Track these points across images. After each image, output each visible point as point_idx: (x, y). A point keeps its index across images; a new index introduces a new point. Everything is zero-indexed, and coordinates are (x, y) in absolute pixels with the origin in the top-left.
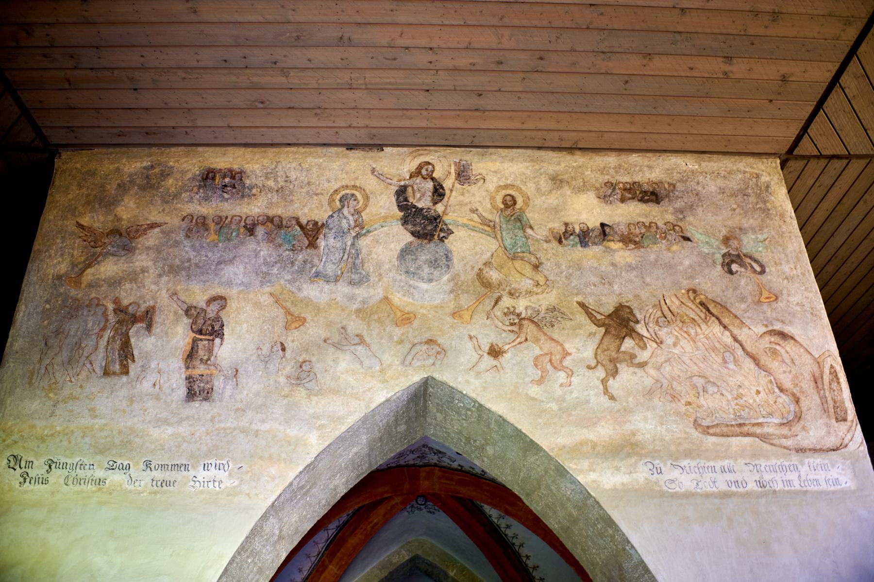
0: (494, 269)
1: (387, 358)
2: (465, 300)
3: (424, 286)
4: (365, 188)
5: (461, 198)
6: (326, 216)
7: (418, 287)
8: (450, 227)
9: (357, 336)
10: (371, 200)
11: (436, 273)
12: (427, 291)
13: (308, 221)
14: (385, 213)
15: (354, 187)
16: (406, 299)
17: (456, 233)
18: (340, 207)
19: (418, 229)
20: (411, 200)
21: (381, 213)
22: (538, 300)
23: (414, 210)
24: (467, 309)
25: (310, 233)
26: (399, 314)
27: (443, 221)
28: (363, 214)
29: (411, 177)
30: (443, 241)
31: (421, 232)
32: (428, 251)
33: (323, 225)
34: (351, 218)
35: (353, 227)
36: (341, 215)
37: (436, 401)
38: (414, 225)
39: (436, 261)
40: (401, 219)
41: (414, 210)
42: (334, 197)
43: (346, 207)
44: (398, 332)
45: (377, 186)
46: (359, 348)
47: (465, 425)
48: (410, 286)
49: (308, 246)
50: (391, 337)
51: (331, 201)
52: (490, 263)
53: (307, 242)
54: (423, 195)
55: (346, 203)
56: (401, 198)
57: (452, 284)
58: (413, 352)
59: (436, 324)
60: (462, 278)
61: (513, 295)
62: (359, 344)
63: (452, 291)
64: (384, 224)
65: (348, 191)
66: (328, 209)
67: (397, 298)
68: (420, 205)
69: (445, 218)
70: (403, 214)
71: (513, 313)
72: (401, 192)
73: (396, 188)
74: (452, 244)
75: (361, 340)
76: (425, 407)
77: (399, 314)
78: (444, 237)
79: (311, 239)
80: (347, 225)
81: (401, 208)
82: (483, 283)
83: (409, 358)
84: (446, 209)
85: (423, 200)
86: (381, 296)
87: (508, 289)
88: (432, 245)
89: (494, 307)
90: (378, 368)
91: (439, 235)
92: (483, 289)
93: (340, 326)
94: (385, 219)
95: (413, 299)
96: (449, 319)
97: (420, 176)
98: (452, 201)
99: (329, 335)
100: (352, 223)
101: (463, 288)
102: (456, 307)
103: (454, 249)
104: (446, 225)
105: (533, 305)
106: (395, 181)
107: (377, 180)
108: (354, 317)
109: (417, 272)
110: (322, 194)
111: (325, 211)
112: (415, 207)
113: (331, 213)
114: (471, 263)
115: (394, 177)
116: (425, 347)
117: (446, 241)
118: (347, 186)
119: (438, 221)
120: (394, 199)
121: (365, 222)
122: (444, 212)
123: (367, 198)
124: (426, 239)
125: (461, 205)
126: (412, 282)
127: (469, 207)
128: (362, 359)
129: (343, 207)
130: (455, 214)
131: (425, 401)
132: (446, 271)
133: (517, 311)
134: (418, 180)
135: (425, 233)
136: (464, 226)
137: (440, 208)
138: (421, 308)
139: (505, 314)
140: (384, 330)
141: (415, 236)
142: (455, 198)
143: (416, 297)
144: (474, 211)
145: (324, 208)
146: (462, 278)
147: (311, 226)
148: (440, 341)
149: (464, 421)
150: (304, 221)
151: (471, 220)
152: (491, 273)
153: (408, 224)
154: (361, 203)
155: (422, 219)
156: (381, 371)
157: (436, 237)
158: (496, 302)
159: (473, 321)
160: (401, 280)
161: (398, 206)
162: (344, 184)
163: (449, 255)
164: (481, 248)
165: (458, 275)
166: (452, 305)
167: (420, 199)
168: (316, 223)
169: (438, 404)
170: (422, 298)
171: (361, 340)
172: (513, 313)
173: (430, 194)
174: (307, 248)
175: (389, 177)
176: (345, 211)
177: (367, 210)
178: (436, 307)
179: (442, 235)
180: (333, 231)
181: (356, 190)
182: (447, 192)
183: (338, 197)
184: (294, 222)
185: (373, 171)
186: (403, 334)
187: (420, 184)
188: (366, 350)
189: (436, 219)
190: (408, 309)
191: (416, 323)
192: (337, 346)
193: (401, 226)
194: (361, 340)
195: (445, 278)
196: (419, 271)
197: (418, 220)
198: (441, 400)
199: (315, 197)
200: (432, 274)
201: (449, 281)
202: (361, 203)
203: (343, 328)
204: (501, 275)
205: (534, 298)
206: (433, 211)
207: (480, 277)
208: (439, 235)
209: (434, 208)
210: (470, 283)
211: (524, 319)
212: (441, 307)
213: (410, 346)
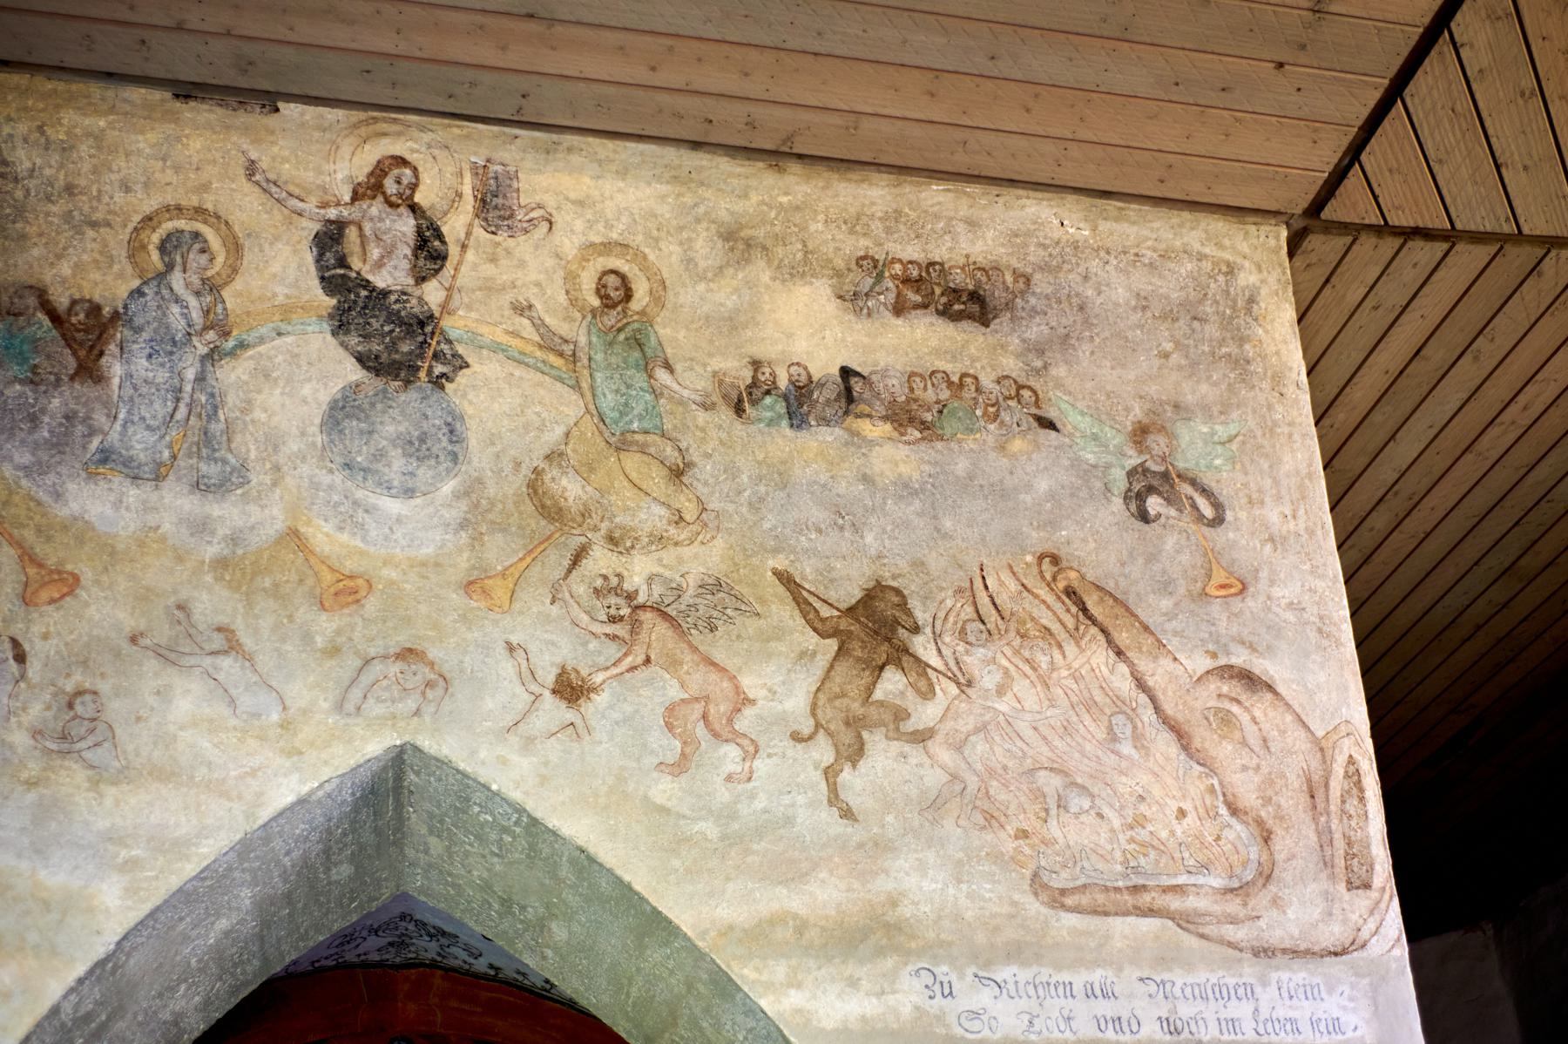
0: (570, 470)
1: (299, 692)
2: (499, 551)
3: (392, 506)
4: (231, 219)
5: (489, 270)
6: (123, 291)
7: (375, 508)
8: (461, 350)
9: (219, 630)
10: (248, 257)
11: (424, 473)
12: (399, 520)
13: (74, 302)
14: (287, 297)
15: (200, 212)
16: (344, 537)
17: (476, 367)
18: (160, 267)
19: (376, 347)
20: (356, 263)
21: (275, 295)
22: (680, 560)
23: (364, 293)
24: (503, 575)
25: (80, 336)
26: (328, 577)
27: (442, 332)
28: (223, 293)
29: (356, 197)
30: (442, 388)
31: (384, 358)
32: (402, 412)
33: (116, 315)
34: (193, 302)
35: (198, 327)
36: (165, 292)
37: (427, 806)
38: (366, 337)
39: (422, 440)
40: (331, 317)
41: (364, 293)
42: (143, 236)
43: (178, 268)
44: (326, 625)
45: (265, 216)
46: (226, 662)
47: (498, 867)
48: (356, 503)
49: (77, 373)
50: (307, 638)
51: (136, 248)
52: (561, 454)
53: (72, 363)
54: (389, 252)
55: (178, 259)
56: (330, 257)
57: (463, 505)
58: (366, 679)
59: (423, 609)
60: (491, 491)
61: (616, 545)
62: (226, 652)
63: (463, 525)
64: (284, 327)
65: (181, 224)
66: (129, 269)
67: (324, 535)
68: (380, 281)
69: (447, 323)
70: (334, 302)
71: (616, 591)
72: (330, 240)
73: (316, 227)
74: (464, 396)
75: (232, 645)
76: (400, 819)
77: (328, 577)
78: (443, 375)
79: (82, 353)
80: (183, 322)
81: (330, 284)
82: (543, 506)
83: (356, 694)
84: (449, 298)
85: (388, 267)
86: (280, 525)
87: (605, 526)
88: (412, 395)
89: (569, 571)
90: (275, 717)
91: (430, 371)
92: (543, 523)
93: (172, 601)
94: (286, 312)
95: (364, 539)
96: (456, 598)
97: (380, 198)
98: (466, 277)
99: (142, 627)
100: (196, 316)
101: (490, 516)
102: (474, 568)
103: (470, 410)
104: (449, 342)
105: (667, 573)
106: (310, 206)
107: (264, 197)
108: (209, 578)
109: (374, 466)
110: (108, 225)
111: (121, 275)
112: (366, 284)
113: (136, 283)
114: (512, 452)
115: (309, 192)
116: (395, 668)
117: (449, 387)
118: (179, 208)
119: (428, 329)
120: (309, 258)
121: (231, 319)
122: (444, 307)
123: (235, 248)
124: (396, 377)
125: (489, 289)
126: (360, 494)
127: (509, 297)
128: (233, 692)
129: (170, 267)
130: (473, 315)
131: (399, 806)
132: (448, 471)
133: (626, 586)
134: (376, 207)
135: (394, 361)
136: (497, 348)
137: (433, 293)
138: (385, 563)
139: (597, 591)
140: (290, 618)
141: (368, 368)
142: (475, 267)
143: (373, 533)
144: (523, 309)
145: (116, 267)
146: (491, 491)
147: (82, 316)
148: (433, 653)
149: (496, 860)
150: (61, 300)
151: (514, 334)
152: (564, 482)
153: (347, 332)
154: (220, 260)
155: (388, 321)
156: (285, 725)
157: (422, 374)
158: (576, 561)
159: (517, 606)
160: (331, 487)
161: (322, 279)
162: (170, 199)
163: (458, 426)
164: (538, 414)
165: (480, 481)
166: (463, 561)
167: (379, 265)
168: (95, 309)
169: (431, 816)
170: (386, 538)
171: (232, 645)
172: (616, 591)
173: (408, 252)
174: (72, 378)
175: (297, 191)
176: (177, 280)
177: (238, 284)
178: (423, 564)
179: (439, 369)
180: (145, 335)
181: (205, 222)
182: (453, 251)
183: (156, 238)
184: (32, 301)
185: (251, 169)
186: (338, 632)
187: (381, 220)
188: (243, 668)
189: (422, 324)
190: (350, 566)
191: (371, 605)
192: (167, 655)
193: (329, 337)
194: (229, 640)
195: (448, 488)
196: (379, 466)
197: (375, 324)
198: (439, 806)
199: (91, 233)
200: (412, 474)
201: (457, 496)
202: (220, 260)
203: (180, 607)
204: (589, 489)
205: (669, 555)
206: (414, 301)
207: (536, 492)
208: (430, 371)
209: (417, 292)
210: (510, 506)
211: (643, 607)
212: (437, 565)
213: (358, 663)
